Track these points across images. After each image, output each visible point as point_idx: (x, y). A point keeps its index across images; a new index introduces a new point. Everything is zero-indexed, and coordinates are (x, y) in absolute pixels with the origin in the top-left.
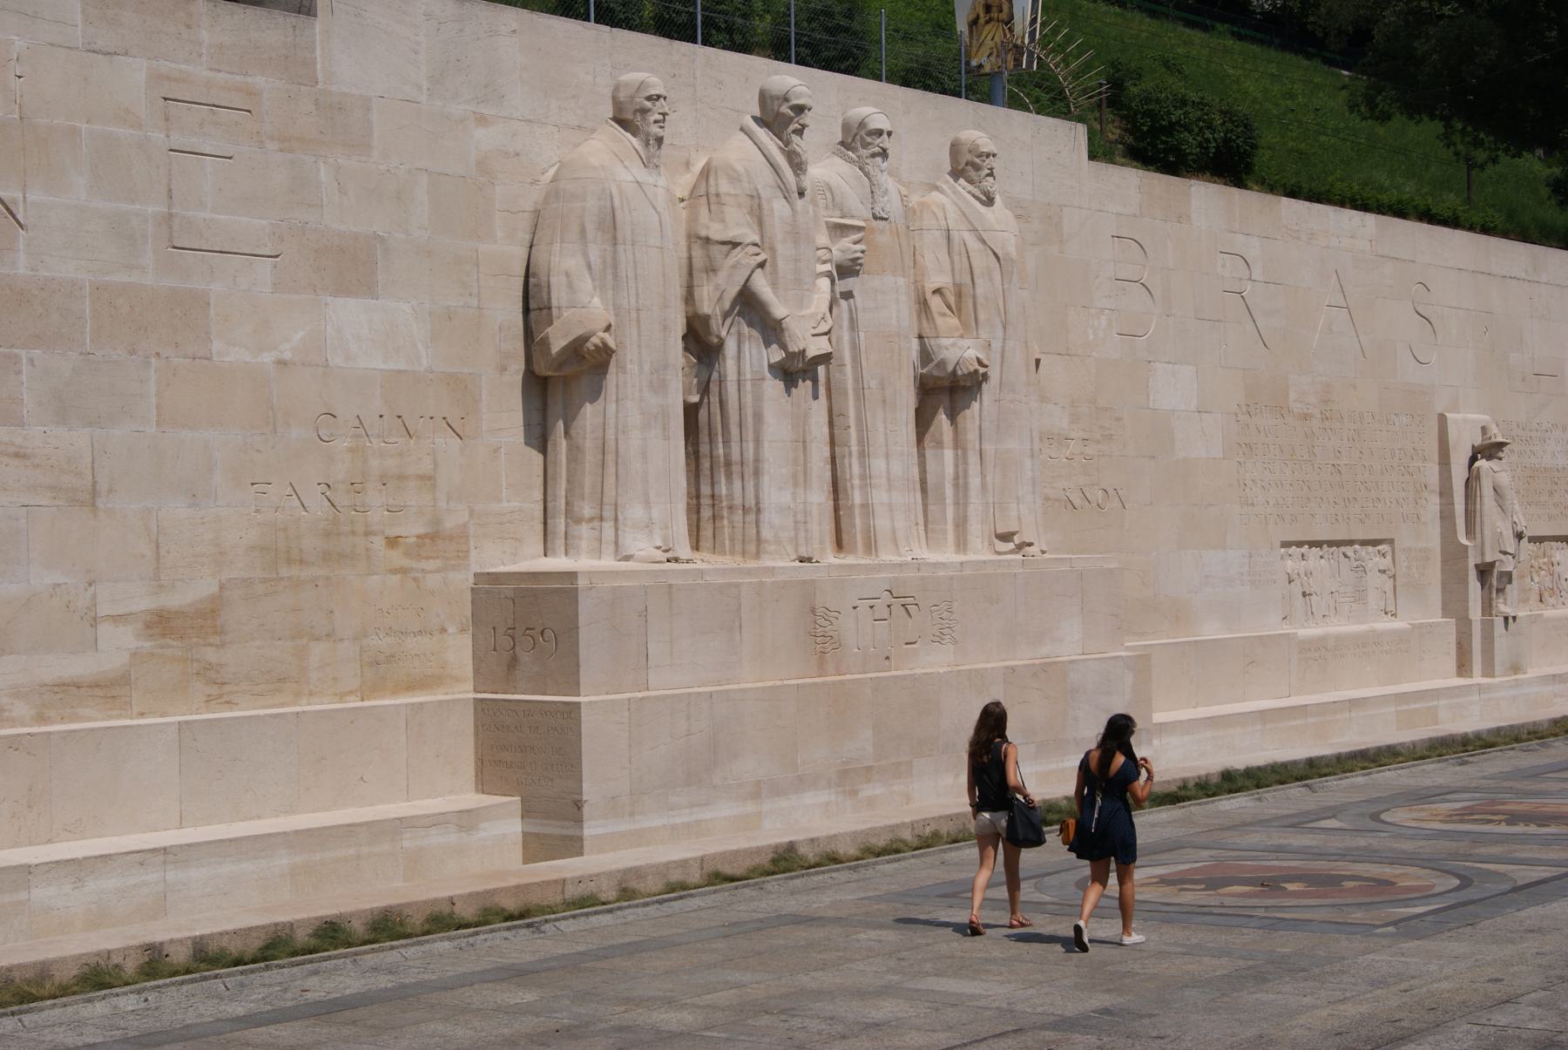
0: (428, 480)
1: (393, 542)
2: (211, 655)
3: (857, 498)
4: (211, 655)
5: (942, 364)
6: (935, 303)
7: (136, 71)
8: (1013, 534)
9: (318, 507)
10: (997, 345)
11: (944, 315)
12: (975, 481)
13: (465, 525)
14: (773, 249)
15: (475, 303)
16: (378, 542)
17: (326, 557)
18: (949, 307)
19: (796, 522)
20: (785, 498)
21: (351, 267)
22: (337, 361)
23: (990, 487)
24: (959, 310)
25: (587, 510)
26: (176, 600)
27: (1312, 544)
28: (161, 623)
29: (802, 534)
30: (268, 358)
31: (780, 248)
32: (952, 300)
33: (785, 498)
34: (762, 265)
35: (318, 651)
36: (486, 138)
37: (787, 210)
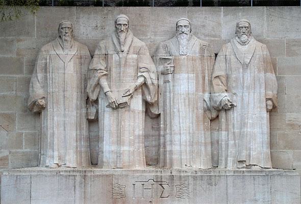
3: (168, 148)
5: (216, 102)
6: (215, 82)
8: (245, 161)
10: (239, 94)
11: (219, 85)
12: (231, 142)
13: (7, 156)
14: (110, 70)
15: (15, 93)
18: (222, 83)
19: (117, 156)
20: (114, 148)
23: (237, 145)
24: (227, 83)
25: (42, 152)
29: (119, 160)
31: (114, 70)
32: (224, 79)
33: (114, 148)
34: (105, 75)
37: (118, 58)
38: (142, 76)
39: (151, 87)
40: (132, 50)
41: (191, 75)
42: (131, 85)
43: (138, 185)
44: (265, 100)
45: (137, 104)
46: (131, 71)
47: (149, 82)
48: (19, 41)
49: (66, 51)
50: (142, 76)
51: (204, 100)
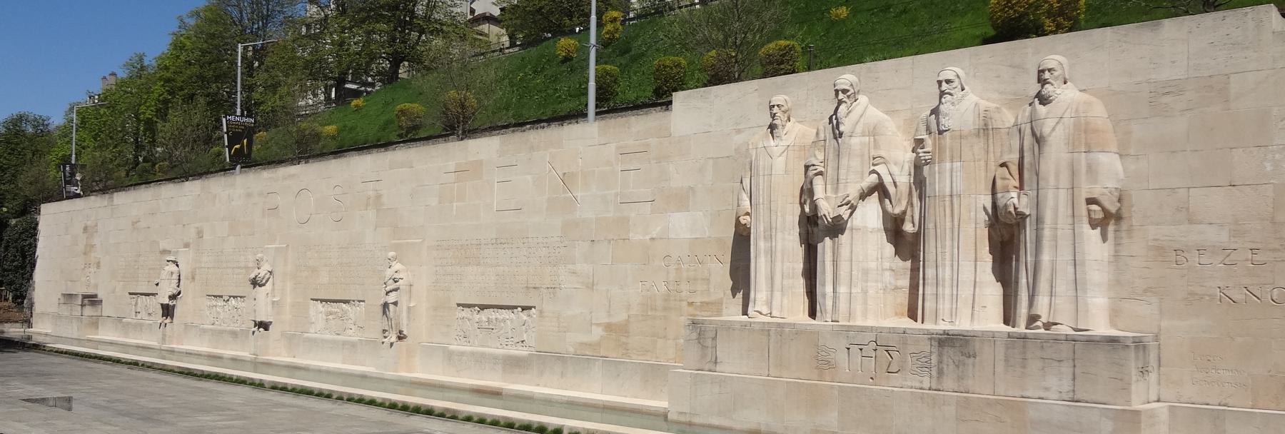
0: (707, 280)
1: (691, 304)
2: (624, 339)
4: (624, 339)
7: (613, 147)
9: (663, 289)
11: (1004, 179)
16: (684, 304)
17: (665, 309)
21: (681, 200)
22: (672, 236)
26: (614, 320)
27: (322, 301)
28: (609, 327)
30: (648, 237)
34: (820, 173)
35: (660, 342)
36: (739, 139)
38: (874, 172)
39: (891, 189)
40: (859, 129)
41: (957, 165)
42: (853, 192)
43: (855, 349)
44: (1084, 202)
45: (870, 215)
46: (855, 163)
47: (887, 180)
48: (739, 131)
49: (777, 141)
50: (874, 172)
51: (985, 209)
